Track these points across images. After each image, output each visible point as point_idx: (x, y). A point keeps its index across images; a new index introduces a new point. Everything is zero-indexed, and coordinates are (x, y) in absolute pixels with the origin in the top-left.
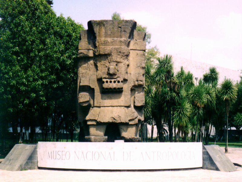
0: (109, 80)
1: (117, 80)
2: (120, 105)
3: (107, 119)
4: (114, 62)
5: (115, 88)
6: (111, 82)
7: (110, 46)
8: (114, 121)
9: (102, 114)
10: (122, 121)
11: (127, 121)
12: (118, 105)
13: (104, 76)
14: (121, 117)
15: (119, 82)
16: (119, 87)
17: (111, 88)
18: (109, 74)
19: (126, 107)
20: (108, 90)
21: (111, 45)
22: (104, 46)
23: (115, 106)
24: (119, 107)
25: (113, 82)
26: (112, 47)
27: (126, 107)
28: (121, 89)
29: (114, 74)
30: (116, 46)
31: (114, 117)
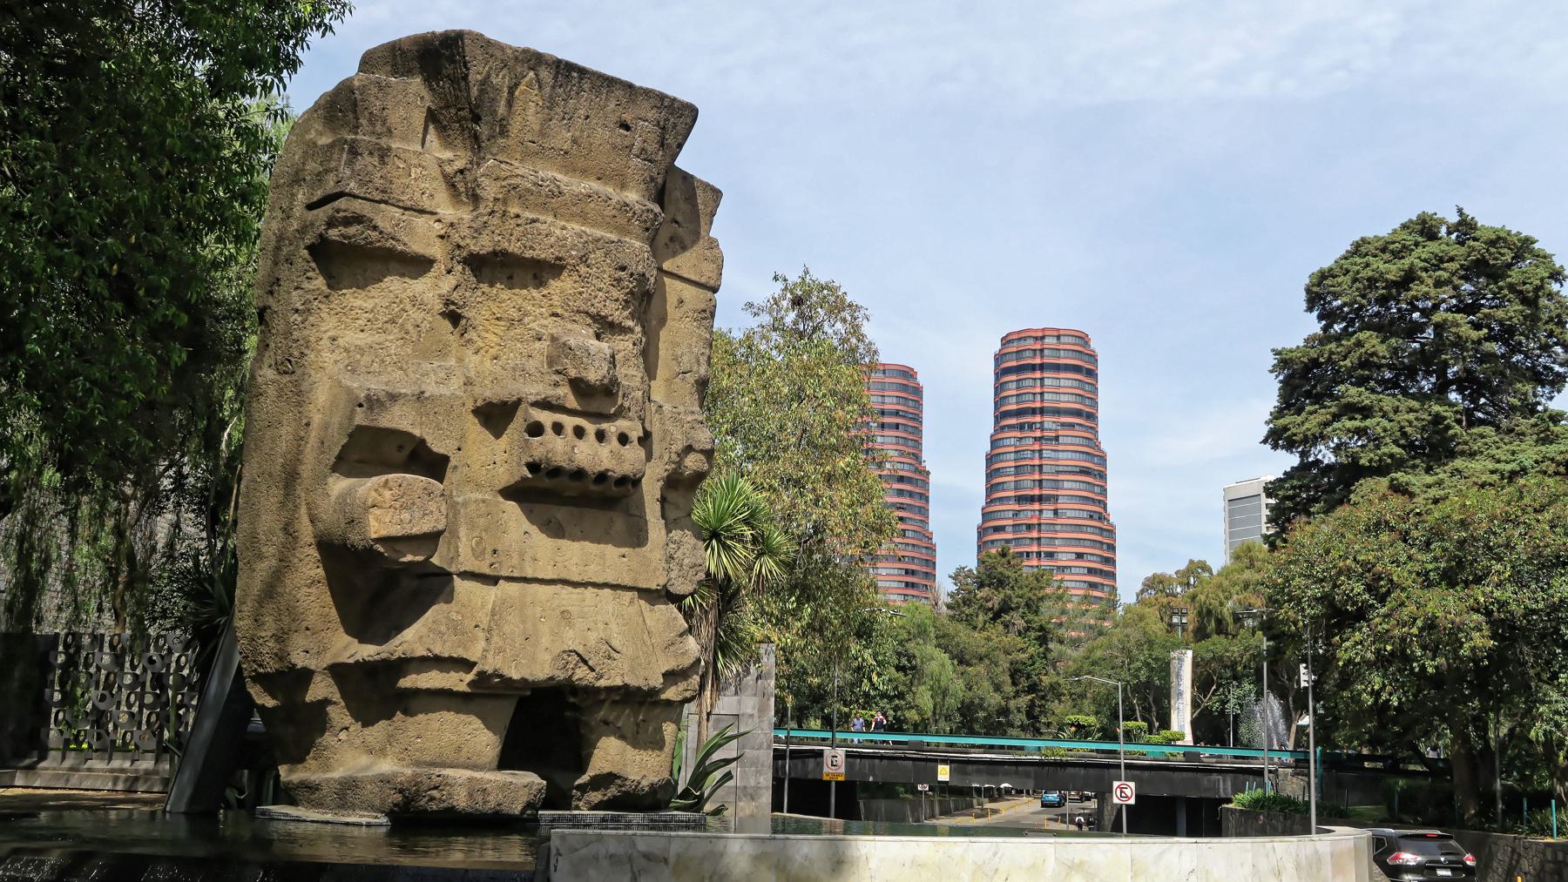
0: (569, 422)
1: (613, 429)
2: (611, 580)
3: (535, 663)
4: (589, 321)
6: (579, 432)
8: (582, 675)
9: (512, 625)
10: (628, 680)
11: (657, 681)
12: (600, 580)
13: (535, 390)
14: (624, 651)
15: (623, 439)
16: (626, 469)
17: (579, 474)
18: (579, 386)
19: (645, 593)
21: (572, 217)
23: (585, 585)
24: (607, 591)
27: (645, 593)
29: (609, 390)
30: (595, 225)
31: (580, 650)
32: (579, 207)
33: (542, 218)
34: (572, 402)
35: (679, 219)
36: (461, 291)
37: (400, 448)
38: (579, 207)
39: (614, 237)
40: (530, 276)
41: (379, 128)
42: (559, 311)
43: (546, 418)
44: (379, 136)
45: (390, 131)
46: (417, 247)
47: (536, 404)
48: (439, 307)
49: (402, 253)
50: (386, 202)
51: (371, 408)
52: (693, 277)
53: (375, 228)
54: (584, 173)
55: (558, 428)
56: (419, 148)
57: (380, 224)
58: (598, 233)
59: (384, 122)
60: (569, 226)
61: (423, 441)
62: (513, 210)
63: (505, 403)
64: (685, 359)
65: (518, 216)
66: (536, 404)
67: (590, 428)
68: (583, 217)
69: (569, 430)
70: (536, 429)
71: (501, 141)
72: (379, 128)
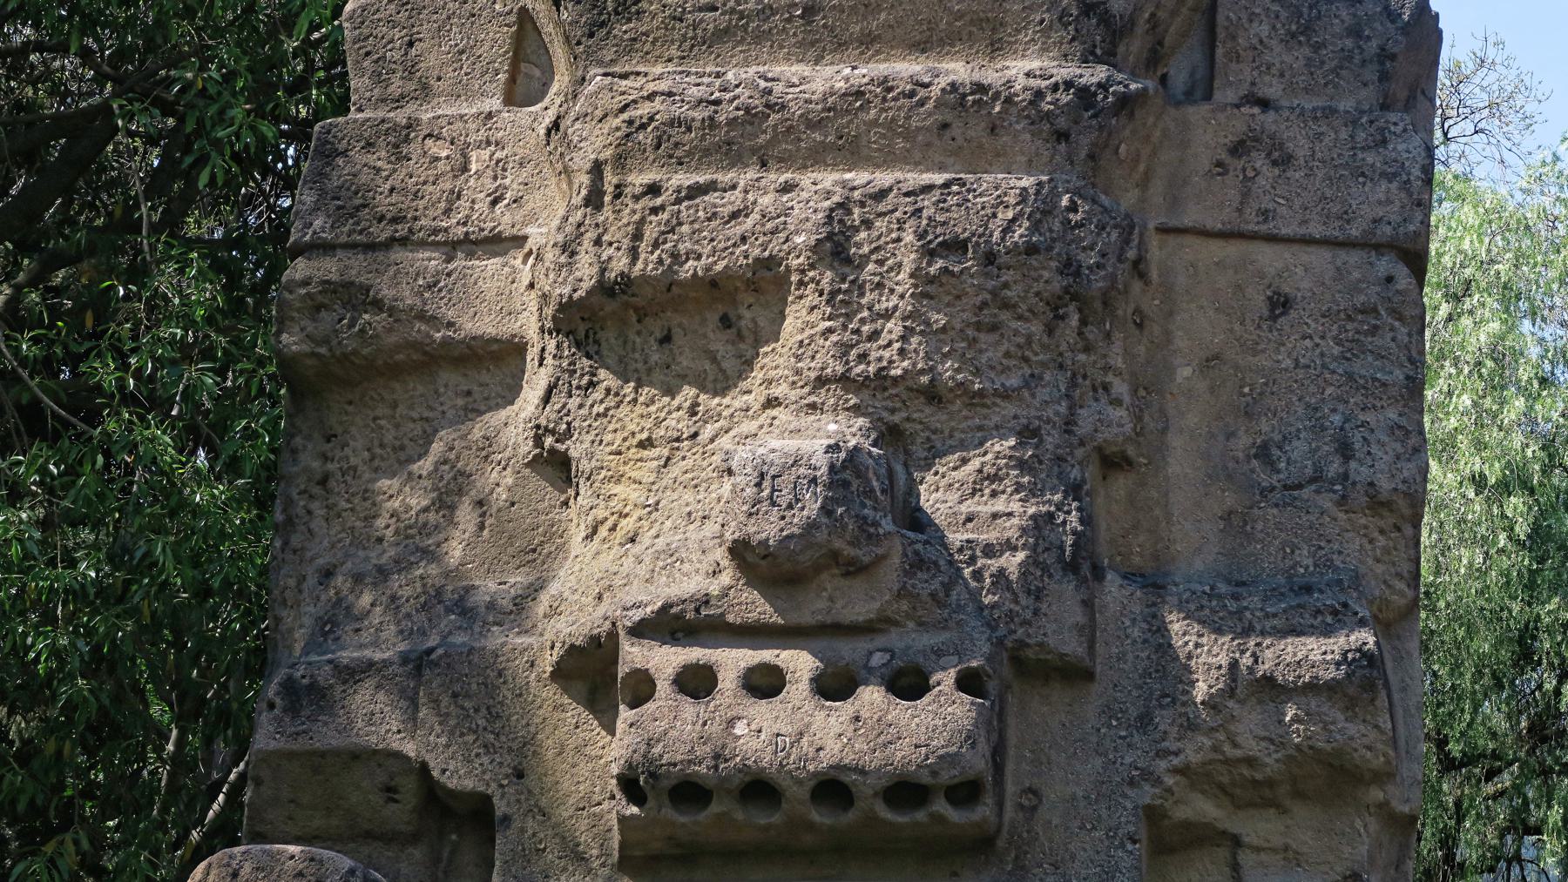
0: (732, 661)
5: (832, 788)
7: (785, 161)
17: (759, 788)
20: (715, 808)
21: (817, 157)
22: (703, 155)
25: (798, 689)
26: (828, 179)
28: (941, 806)
30: (888, 160)
32: (835, 133)
33: (725, 178)
34: (755, 606)
35: (1272, 89)
36: (557, 401)
37: (390, 791)
38: (835, 133)
39: (939, 178)
40: (713, 318)
41: (396, 86)
42: (779, 391)
43: (665, 660)
44: (399, 101)
45: (425, 87)
46: (482, 324)
47: (640, 631)
48: (527, 448)
49: (446, 342)
50: (404, 242)
51: (293, 709)
52: (1316, 230)
53: (378, 305)
54: (869, 44)
55: (696, 682)
56: (495, 103)
57: (387, 293)
58: (884, 178)
59: (411, 71)
60: (806, 179)
61: (424, 768)
62: (639, 180)
63: (595, 640)
64: (1298, 449)
65: (654, 189)
66: (640, 631)
67: (800, 663)
68: (850, 152)
69: (728, 680)
70: (641, 688)
71: (621, 29)
72: (396, 86)
